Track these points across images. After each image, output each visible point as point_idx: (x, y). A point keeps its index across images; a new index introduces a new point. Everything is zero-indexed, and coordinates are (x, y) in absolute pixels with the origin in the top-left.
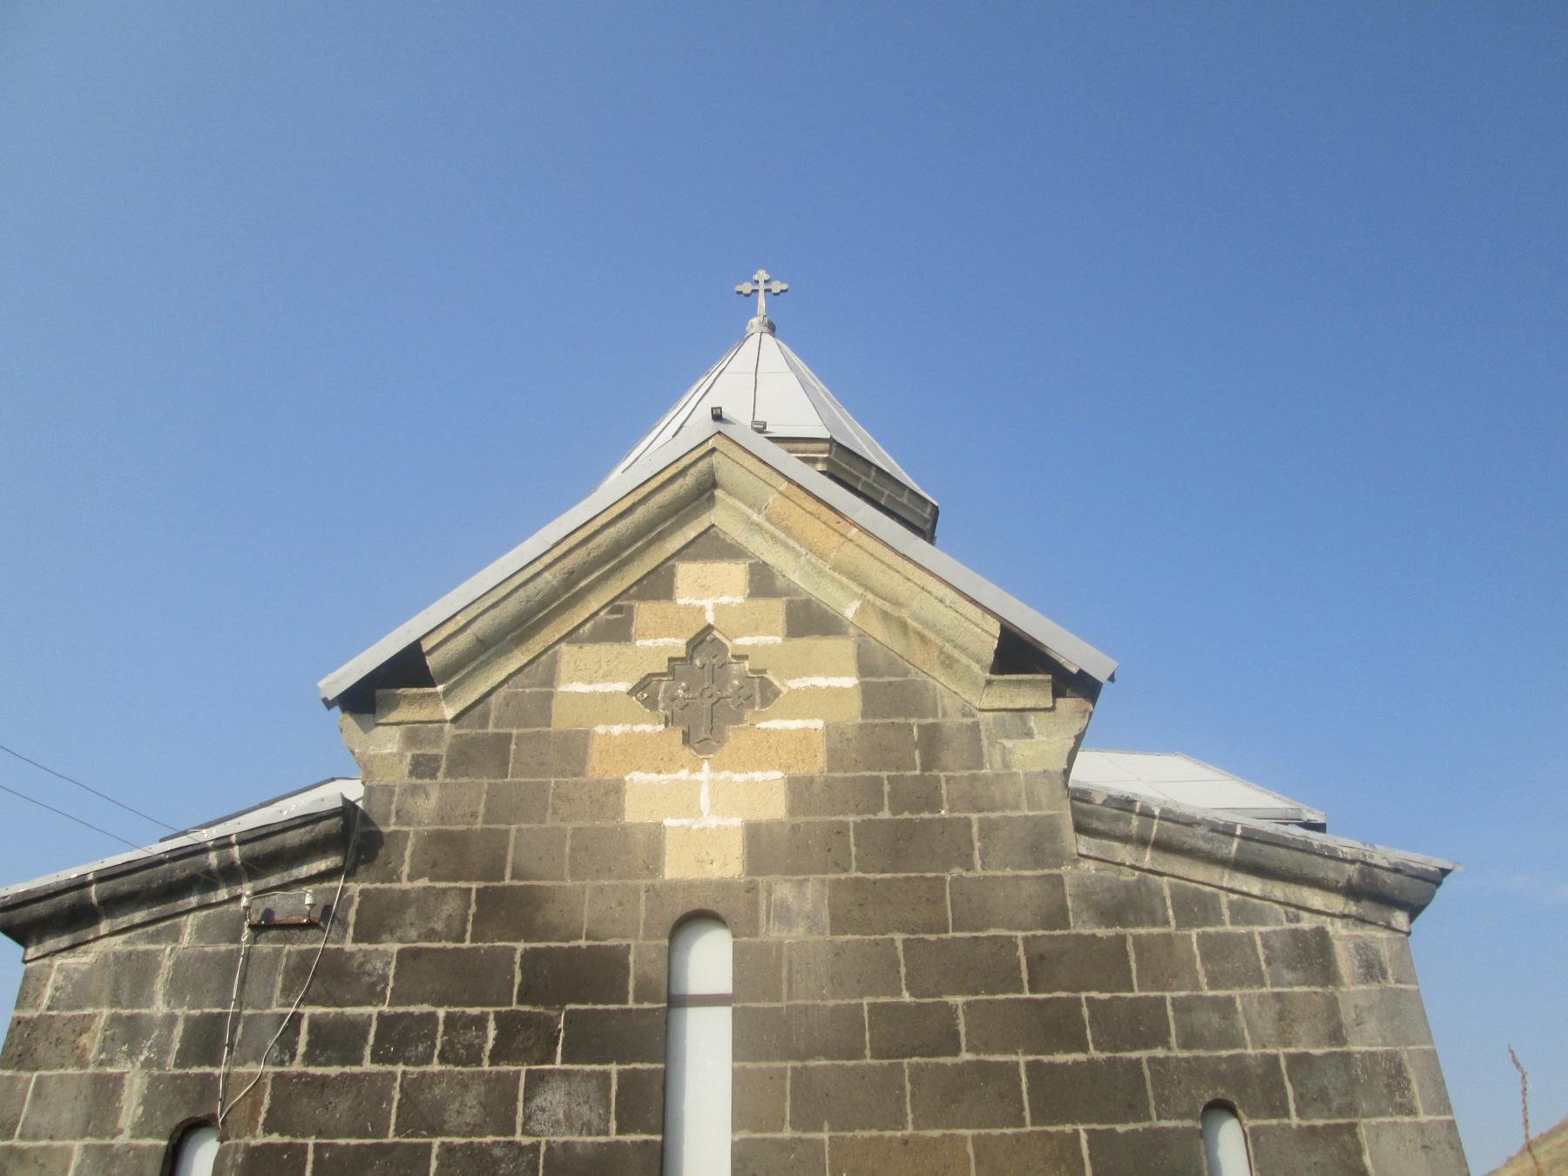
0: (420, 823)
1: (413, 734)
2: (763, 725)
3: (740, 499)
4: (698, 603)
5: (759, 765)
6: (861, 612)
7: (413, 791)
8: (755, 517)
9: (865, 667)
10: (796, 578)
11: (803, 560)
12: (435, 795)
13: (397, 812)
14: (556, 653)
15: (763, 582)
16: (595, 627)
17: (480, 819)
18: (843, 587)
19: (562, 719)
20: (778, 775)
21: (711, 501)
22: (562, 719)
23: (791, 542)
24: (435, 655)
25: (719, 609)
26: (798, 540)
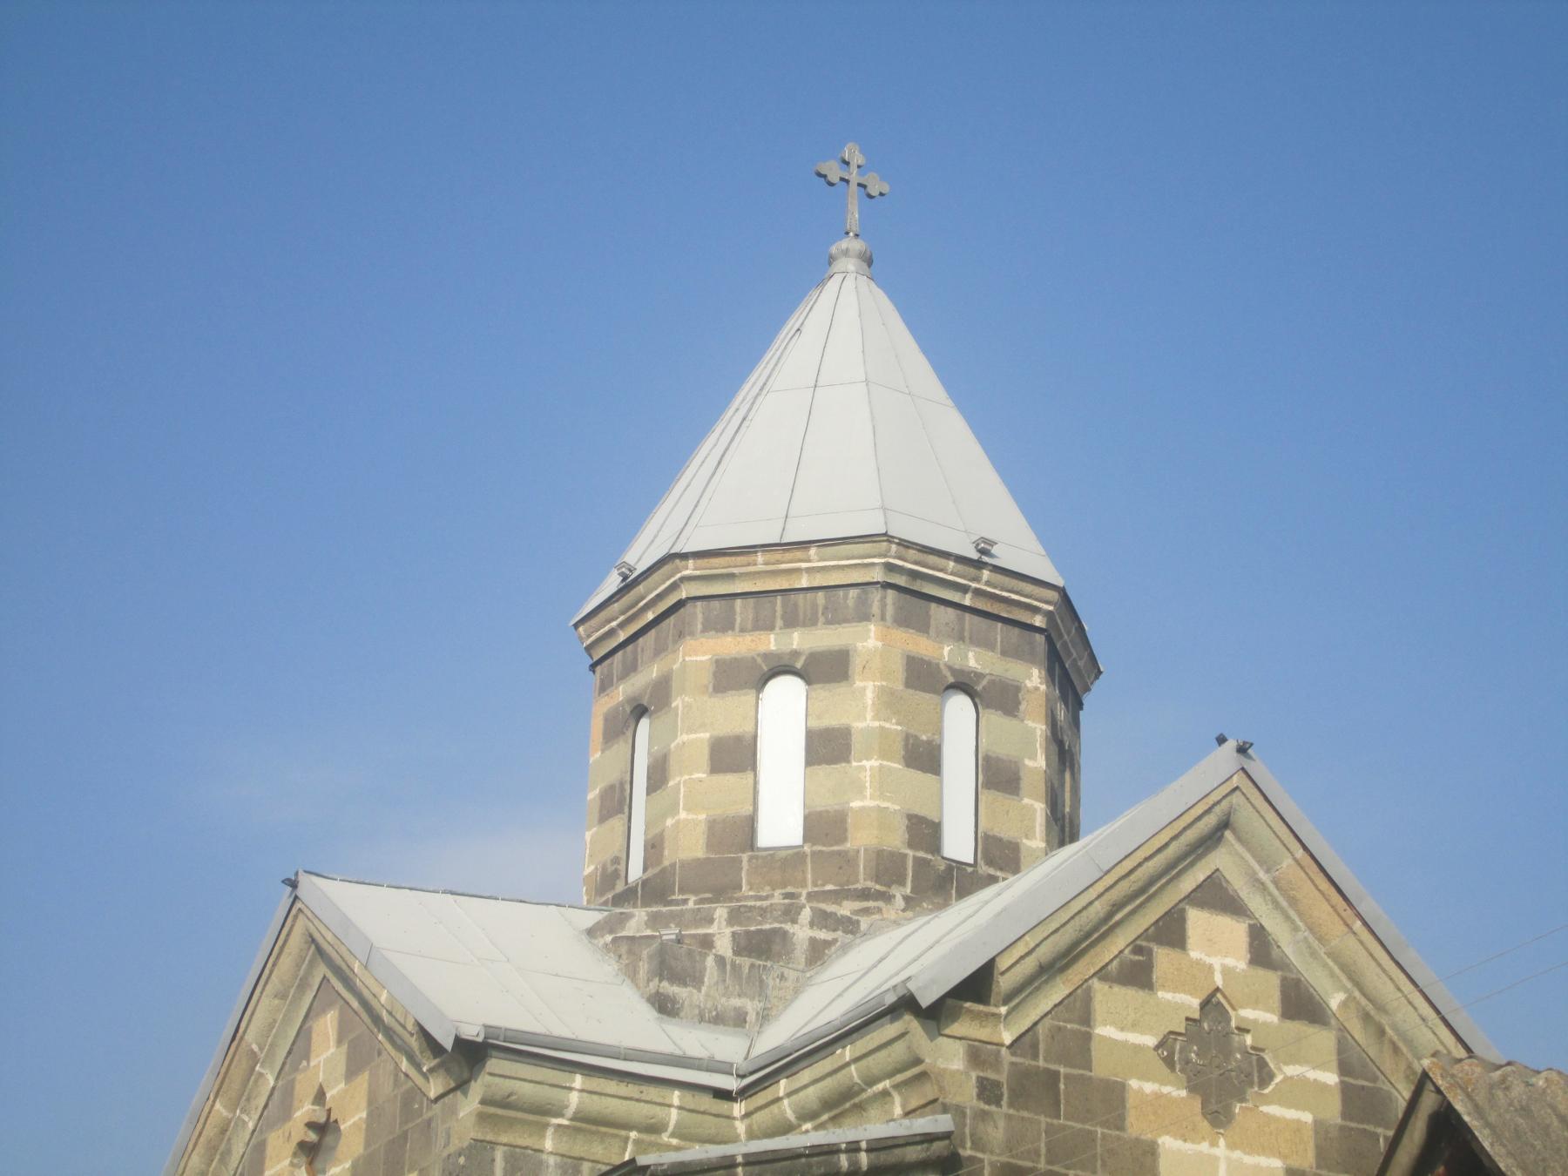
0: (992, 1152)
1: (978, 1055)
2: (1264, 1109)
3: (1249, 850)
4: (1208, 960)
5: (1264, 1150)
6: (1344, 1004)
7: (983, 1116)
8: (1262, 875)
9: (1344, 1068)
10: (1289, 950)
11: (1300, 935)
12: (1001, 1124)
13: (972, 1135)
14: (1089, 988)
15: (1261, 950)
16: (1121, 964)
17: (1043, 1159)
18: (1332, 975)
19: (1102, 1067)
20: (1277, 1163)
21: (1220, 839)
22: (1102, 1067)
23: (1292, 913)
24: (1007, 975)
25: (1226, 971)
26: (1300, 914)
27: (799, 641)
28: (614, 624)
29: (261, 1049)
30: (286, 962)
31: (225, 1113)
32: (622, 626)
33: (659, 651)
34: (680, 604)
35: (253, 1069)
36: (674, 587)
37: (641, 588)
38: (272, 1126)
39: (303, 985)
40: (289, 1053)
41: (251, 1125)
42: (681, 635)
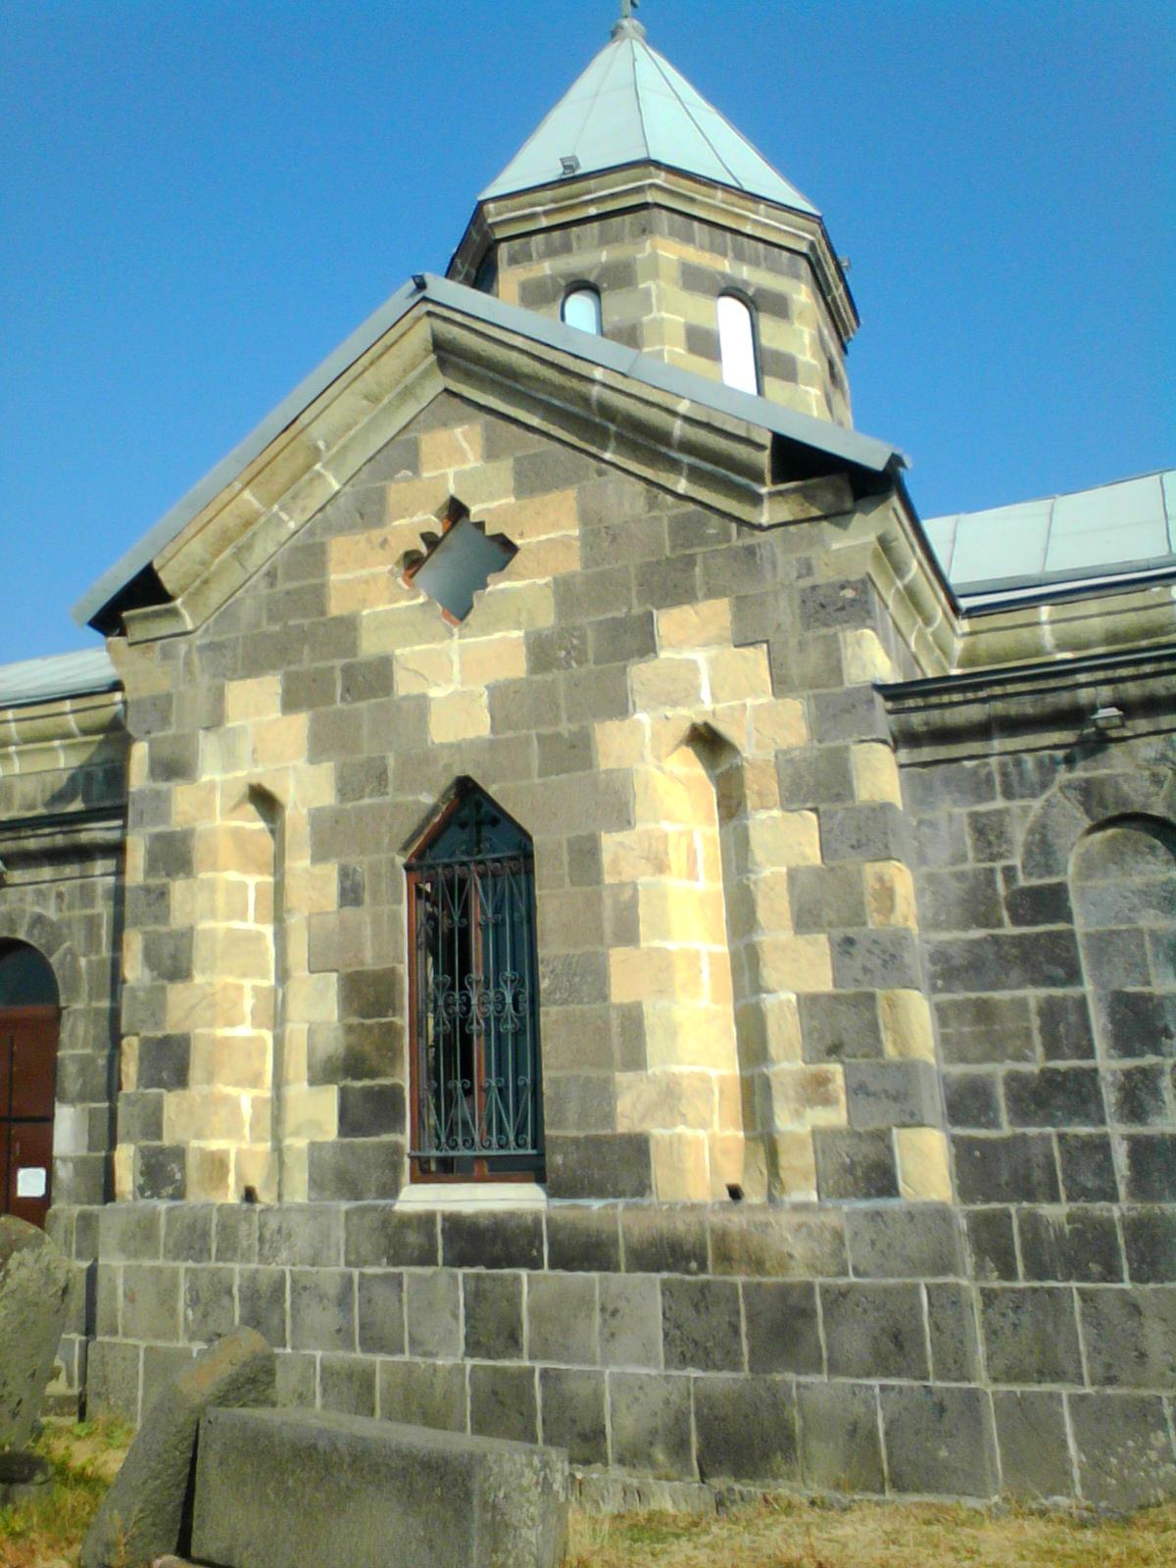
27: (750, 275)
28: (539, 209)
29: (328, 447)
30: (390, 365)
31: (256, 504)
32: (546, 213)
33: (604, 241)
34: (645, 206)
35: (308, 467)
36: (639, 190)
37: (592, 183)
38: (331, 528)
39: (406, 394)
40: (370, 460)
41: (292, 525)
42: (645, 231)
